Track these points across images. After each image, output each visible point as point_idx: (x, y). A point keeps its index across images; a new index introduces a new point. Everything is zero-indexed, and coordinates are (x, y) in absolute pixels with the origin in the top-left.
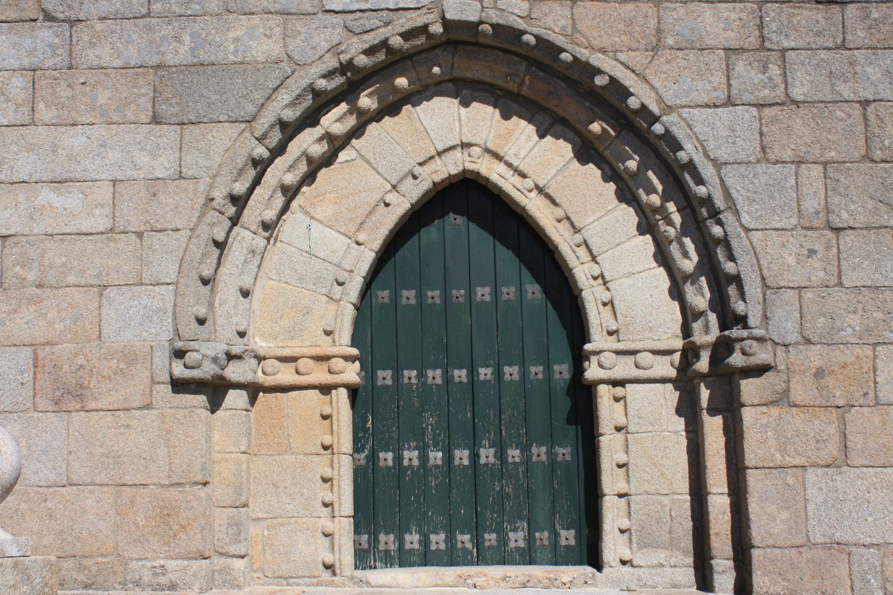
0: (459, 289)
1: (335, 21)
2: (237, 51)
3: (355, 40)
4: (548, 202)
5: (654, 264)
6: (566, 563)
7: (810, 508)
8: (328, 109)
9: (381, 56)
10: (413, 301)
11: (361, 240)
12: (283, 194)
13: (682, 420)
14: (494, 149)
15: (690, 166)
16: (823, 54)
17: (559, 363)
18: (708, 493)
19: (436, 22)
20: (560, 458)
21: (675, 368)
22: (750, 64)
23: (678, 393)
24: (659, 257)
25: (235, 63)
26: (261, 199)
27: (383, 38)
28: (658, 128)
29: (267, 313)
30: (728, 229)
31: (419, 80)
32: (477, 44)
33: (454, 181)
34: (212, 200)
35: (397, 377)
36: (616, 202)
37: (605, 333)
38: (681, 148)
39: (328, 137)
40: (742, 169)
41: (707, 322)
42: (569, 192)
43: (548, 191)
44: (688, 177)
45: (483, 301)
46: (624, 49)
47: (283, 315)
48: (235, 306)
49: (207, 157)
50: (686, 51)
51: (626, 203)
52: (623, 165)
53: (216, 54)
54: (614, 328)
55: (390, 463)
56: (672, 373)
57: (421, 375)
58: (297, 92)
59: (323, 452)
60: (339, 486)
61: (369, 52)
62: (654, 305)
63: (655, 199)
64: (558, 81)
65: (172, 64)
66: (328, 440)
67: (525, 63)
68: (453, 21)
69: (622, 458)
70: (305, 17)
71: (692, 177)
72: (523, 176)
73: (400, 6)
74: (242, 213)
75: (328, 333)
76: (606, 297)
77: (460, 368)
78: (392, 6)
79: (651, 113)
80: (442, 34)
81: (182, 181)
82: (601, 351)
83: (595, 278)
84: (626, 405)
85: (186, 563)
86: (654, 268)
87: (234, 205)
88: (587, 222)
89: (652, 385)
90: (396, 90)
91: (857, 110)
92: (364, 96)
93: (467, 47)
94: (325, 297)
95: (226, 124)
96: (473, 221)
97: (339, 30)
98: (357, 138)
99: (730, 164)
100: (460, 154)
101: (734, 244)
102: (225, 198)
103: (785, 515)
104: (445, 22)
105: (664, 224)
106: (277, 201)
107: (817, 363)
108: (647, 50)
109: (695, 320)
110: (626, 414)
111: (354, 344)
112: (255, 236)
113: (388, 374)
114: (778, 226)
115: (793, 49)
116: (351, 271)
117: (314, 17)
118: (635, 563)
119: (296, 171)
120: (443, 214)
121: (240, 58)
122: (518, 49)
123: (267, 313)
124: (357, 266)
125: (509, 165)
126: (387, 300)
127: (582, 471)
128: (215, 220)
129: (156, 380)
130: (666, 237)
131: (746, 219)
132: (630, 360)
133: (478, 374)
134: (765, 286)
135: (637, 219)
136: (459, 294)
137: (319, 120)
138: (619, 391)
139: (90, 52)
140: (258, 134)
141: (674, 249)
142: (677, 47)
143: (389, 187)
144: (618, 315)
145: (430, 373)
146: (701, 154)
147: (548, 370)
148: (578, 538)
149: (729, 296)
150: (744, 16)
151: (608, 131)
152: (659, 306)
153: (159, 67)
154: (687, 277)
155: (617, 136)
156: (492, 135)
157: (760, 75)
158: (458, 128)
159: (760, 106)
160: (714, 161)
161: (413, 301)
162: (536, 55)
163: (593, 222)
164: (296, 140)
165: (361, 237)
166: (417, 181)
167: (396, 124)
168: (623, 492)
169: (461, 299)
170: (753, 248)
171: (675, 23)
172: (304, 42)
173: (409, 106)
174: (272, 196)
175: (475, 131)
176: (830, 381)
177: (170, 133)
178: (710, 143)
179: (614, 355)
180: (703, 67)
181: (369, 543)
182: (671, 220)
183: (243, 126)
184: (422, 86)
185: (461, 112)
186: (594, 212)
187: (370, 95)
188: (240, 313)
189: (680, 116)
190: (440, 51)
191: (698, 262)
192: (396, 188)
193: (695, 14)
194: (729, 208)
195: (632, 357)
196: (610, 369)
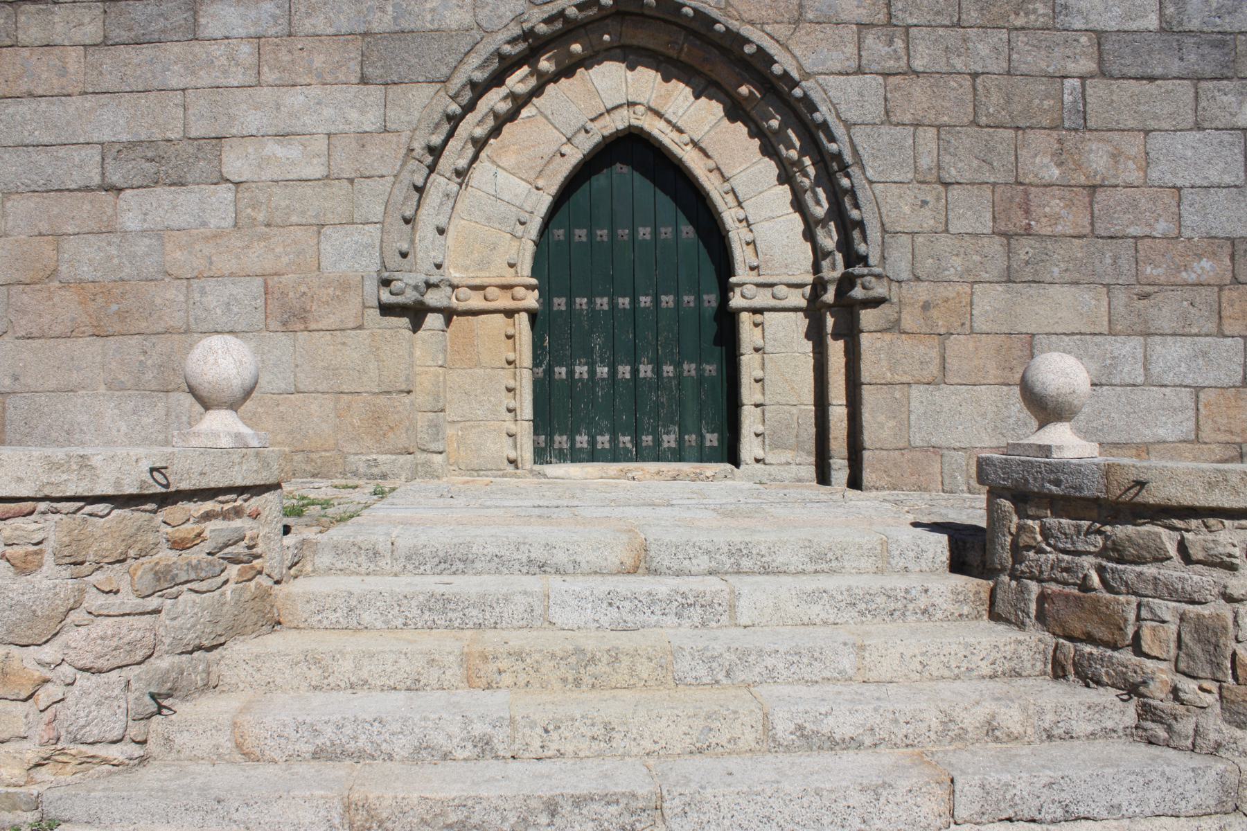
0: (624, 229)
3: (536, 10)
4: (701, 155)
5: (791, 210)
6: (709, 461)
7: (912, 417)
9: (558, 25)
10: (584, 239)
11: (540, 186)
13: (810, 344)
14: (656, 108)
15: (825, 126)
16: (941, 31)
17: (707, 293)
18: (830, 405)
20: (707, 374)
22: (878, 38)
23: (807, 320)
28: (797, 92)
30: (855, 181)
32: (643, 15)
34: (413, 150)
35: (570, 303)
37: (747, 268)
38: (817, 110)
39: (512, 96)
40: (868, 129)
41: (834, 260)
43: (701, 145)
49: (408, 113)
50: (824, 25)
54: (755, 264)
55: (564, 376)
56: (804, 303)
57: (590, 302)
59: (507, 366)
60: (521, 395)
63: (793, 154)
65: (377, 31)
66: (511, 356)
67: (683, 33)
69: (759, 374)
71: (826, 136)
72: (681, 131)
75: (511, 266)
76: (749, 237)
77: (624, 296)
79: (792, 79)
80: (612, 6)
81: (387, 134)
83: (740, 221)
84: (763, 330)
85: (394, 457)
88: (735, 172)
90: (571, 55)
91: (967, 82)
95: (424, 85)
98: (538, 97)
101: (860, 194)
102: (423, 149)
103: (891, 423)
107: (924, 297)
108: (790, 23)
109: (824, 259)
110: (763, 338)
111: (533, 275)
113: (563, 300)
114: (897, 179)
115: (915, 26)
116: (532, 213)
118: (767, 461)
120: (610, 164)
121: (436, 26)
122: (678, 20)
125: (669, 122)
126: (562, 238)
127: (725, 384)
129: (367, 305)
131: (870, 173)
132: (768, 291)
133: (639, 302)
134: (884, 230)
136: (624, 233)
138: (758, 318)
139: (306, 21)
140: (452, 93)
141: (808, 197)
143: (564, 140)
145: (598, 301)
147: (699, 299)
148: (721, 440)
149: (853, 239)
153: (365, 34)
155: (762, 98)
156: (654, 95)
157: (886, 48)
159: (886, 75)
160: (845, 122)
161: (584, 239)
162: (694, 25)
165: (540, 183)
168: (758, 402)
169: (625, 238)
173: (583, 69)
176: (934, 313)
177: (375, 92)
180: (838, 39)
181: (546, 442)
183: (439, 86)
186: (741, 164)
187: (548, 59)
189: (817, 82)
195: (770, 289)
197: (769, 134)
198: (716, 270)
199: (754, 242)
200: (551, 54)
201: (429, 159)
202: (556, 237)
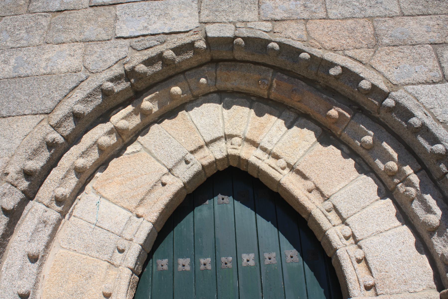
1: (123, 43)
2: (47, 66)
3: (138, 54)
4: (298, 177)
5: (398, 223)
8: (117, 110)
9: (158, 67)
10: (188, 268)
11: (140, 213)
12: (77, 176)
14: (251, 138)
19: (201, 40)
24: (401, 216)
25: (45, 74)
26: (56, 178)
27: (159, 52)
28: (389, 102)
29: (55, 278)
31: (190, 90)
32: (234, 60)
33: (221, 169)
34: (7, 174)
36: (357, 174)
38: (413, 115)
43: (298, 168)
44: (421, 140)
45: (248, 266)
46: (350, 48)
47: (68, 279)
48: (21, 270)
50: (400, 47)
51: (365, 174)
52: (360, 142)
53: (31, 70)
58: (88, 92)
61: (149, 62)
62: (404, 259)
63: (393, 165)
64: (299, 81)
67: (271, 71)
68: (214, 38)
70: (101, 42)
71: (426, 139)
72: (277, 157)
73: (172, 31)
74: (38, 189)
76: (359, 254)
78: (167, 31)
79: (381, 91)
83: (347, 238)
86: (398, 226)
87: (27, 180)
88: (334, 191)
90: (172, 97)
92: (146, 100)
93: (226, 63)
94: (106, 263)
95: (29, 117)
96: (238, 200)
97: (126, 49)
98: (142, 136)
100: (225, 144)
102: (18, 173)
104: (207, 39)
105: (403, 186)
106: (71, 181)
108: (369, 48)
112: (48, 209)
116: (131, 240)
117: (108, 42)
119: (89, 158)
120: (212, 196)
121: (48, 70)
123: (55, 278)
124: (136, 236)
125: (264, 150)
126: (165, 267)
128: (6, 191)
130: (408, 196)
135: (376, 186)
137: (110, 118)
140: (53, 122)
141: (416, 206)
142: (393, 44)
143: (166, 170)
144: (373, 271)
146: (431, 119)
150: (440, 22)
151: (344, 115)
152: (410, 261)
154: (432, 231)
155: (352, 118)
156: (249, 128)
158: (222, 125)
161: (188, 268)
163: (339, 190)
164: (90, 133)
165: (140, 211)
166: (189, 165)
167: (173, 124)
169: (229, 265)
171: (387, 29)
172: (98, 58)
174: (65, 177)
175: (235, 126)
178: (437, 110)
180: (418, 56)
182: (410, 181)
183: (42, 117)
184: (193, 96)
185: (224, 112)
186: (339, 182)
187: (151, 100)
188: (26, 276)
189: (406, 91)
190: (206, 68)
191: (442, 215)
192: (172, 172)
193: (402, 24)
197: (362, 152)
198: (325, 293)
199: (365, 259)
200: (153, 95)
201: (25, 184)
202: (160, 267)
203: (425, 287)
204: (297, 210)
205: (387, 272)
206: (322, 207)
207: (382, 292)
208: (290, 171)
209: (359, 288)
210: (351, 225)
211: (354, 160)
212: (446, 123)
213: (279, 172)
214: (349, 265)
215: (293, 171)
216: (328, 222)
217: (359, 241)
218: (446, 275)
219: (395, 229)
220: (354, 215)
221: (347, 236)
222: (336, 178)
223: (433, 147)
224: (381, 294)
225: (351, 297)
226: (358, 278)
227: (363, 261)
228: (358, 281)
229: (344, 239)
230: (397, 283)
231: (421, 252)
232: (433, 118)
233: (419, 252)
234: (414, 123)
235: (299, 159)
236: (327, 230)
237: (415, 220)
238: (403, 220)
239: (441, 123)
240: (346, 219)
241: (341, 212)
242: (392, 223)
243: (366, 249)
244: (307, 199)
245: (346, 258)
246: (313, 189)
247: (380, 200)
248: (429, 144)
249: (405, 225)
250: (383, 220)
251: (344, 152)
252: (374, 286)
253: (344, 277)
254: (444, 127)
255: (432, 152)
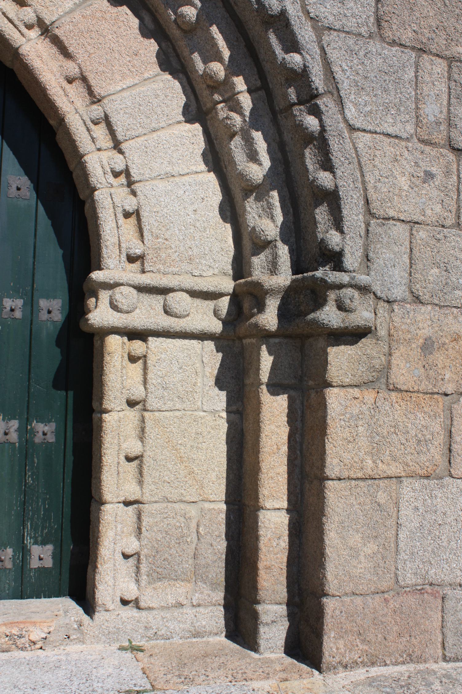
4: (54, 50)
5: (203, 167)
6: (37, 595)
13: (223, 395)
17: (47, 297)
18: (258, 508)
20: (39, 438)
21: (219, 319)
23: (220, 355)
24: (210, 157)
36: (157, 69)
37: (124, 258)
40: (351, 41)
41: (275, 256)
42: (89, 40)
43: (57, 32)
51: (170, 74)
52: (175, 13)
54: (138, 252)
56: (217, 327)
62: (198, 225)
69: (135, 448)
71: (281, 40)
76: (130, 204)
82: (117, 285)
83: (116, 175)
84: (145, 369)
86: (202, 172)
88: (112, 89)
89: (186, 342)
99: (335, 30)
101: (334, 144)
103: (371, 548)
105: (226, 109)
107: (426, 332)
109: (256, 253)
110: (145, 382)
114: (390, 130)
118: (142, 604)
127: (70, 458)
130: (228, 127)
131: (351, 112)
132: (157, 301)
134: (369, 213)
135: (184, 98)
138: (138, 347)
144: (146, 233)
148: (57, 557)
149: (315, 223)
152: (205, 229)
160: (314, 20)
163: (120, 91)
168: (132, 498)
170: (358, 156)
176: (439, 358)
179: (135, 292)
182: (238, 103)
191: (269, 169)
194: (330, 92)
195: (160, 298)
196: (128, 312)
197: (175, 33)
198: (64, 256)
199: (137, 213)
203: (216, 271)
204: (42, 110)
205: (166, 239)
206: (85, 114)
207: (152, 269)
208: (41, 35)
209: (118, 257)
210: (127, 155)
211: (159, 45)
212: (318, 21)
213: (20, 31)
214: (110, 219)
215: (46, 37)
216: (91, 142)
217: (134, 182)
218: (250, 259)
219: (196, 176)
220: (136, 139)
221: (117, 171)
222: (121, 69)
223: (286, 56)
224: (149, 271)
225: (102, 269)
226: (119, 241)
227: (134, 217)
228: (120, 245)
229: (111, 174)
230: (178, 259)
231: (224, 218)
232: (302, 7)
233: (222, 218)
234: (269, 4)
235: (62, 16)
236: (85, 155)
237: (229, 168)
238: (211, 164)
239: (311, 18)
240: (122, 142)
241: (115, 128)
242: (195, 165)
243: (142, 197)
244: (61, 92)
245: (107, 207)
246: (77, 79)
247: (184, 124)
248: (283, 50)
249: (212, 173)
250: (181, 158)
251: (144, 25)
252: (143, 258)
253: (98, 236)
254: (313, 28)
255: (284, 64)
